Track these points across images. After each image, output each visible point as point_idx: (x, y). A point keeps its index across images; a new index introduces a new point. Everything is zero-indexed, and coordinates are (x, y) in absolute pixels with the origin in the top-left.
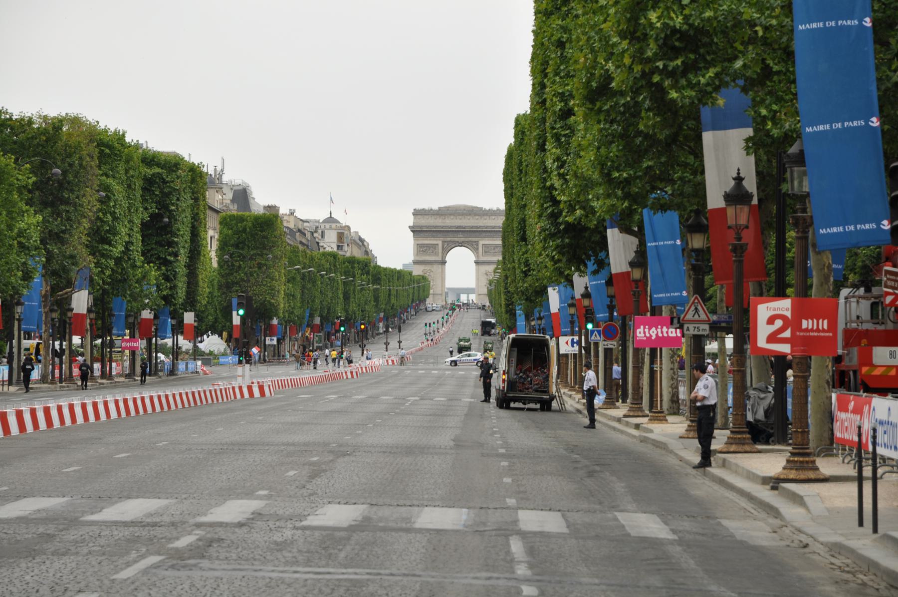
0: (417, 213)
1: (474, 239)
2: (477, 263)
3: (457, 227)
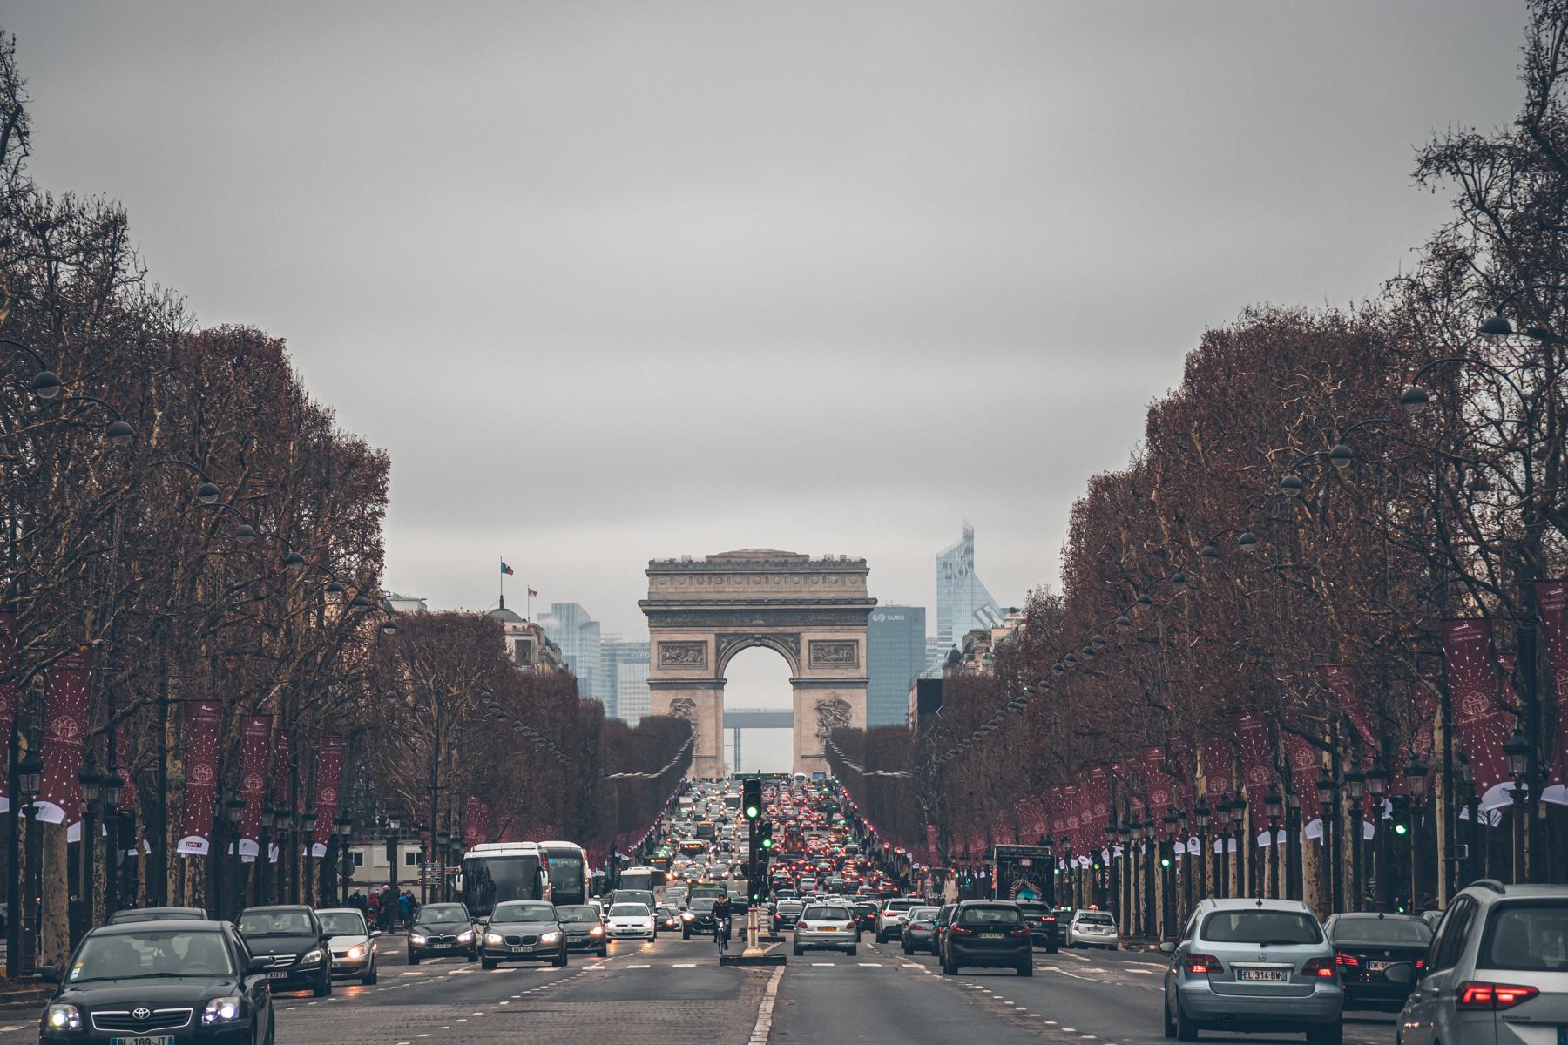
0: (657, 570)
1: (789, 630)
2: (797, 684)
3: (751, 602)
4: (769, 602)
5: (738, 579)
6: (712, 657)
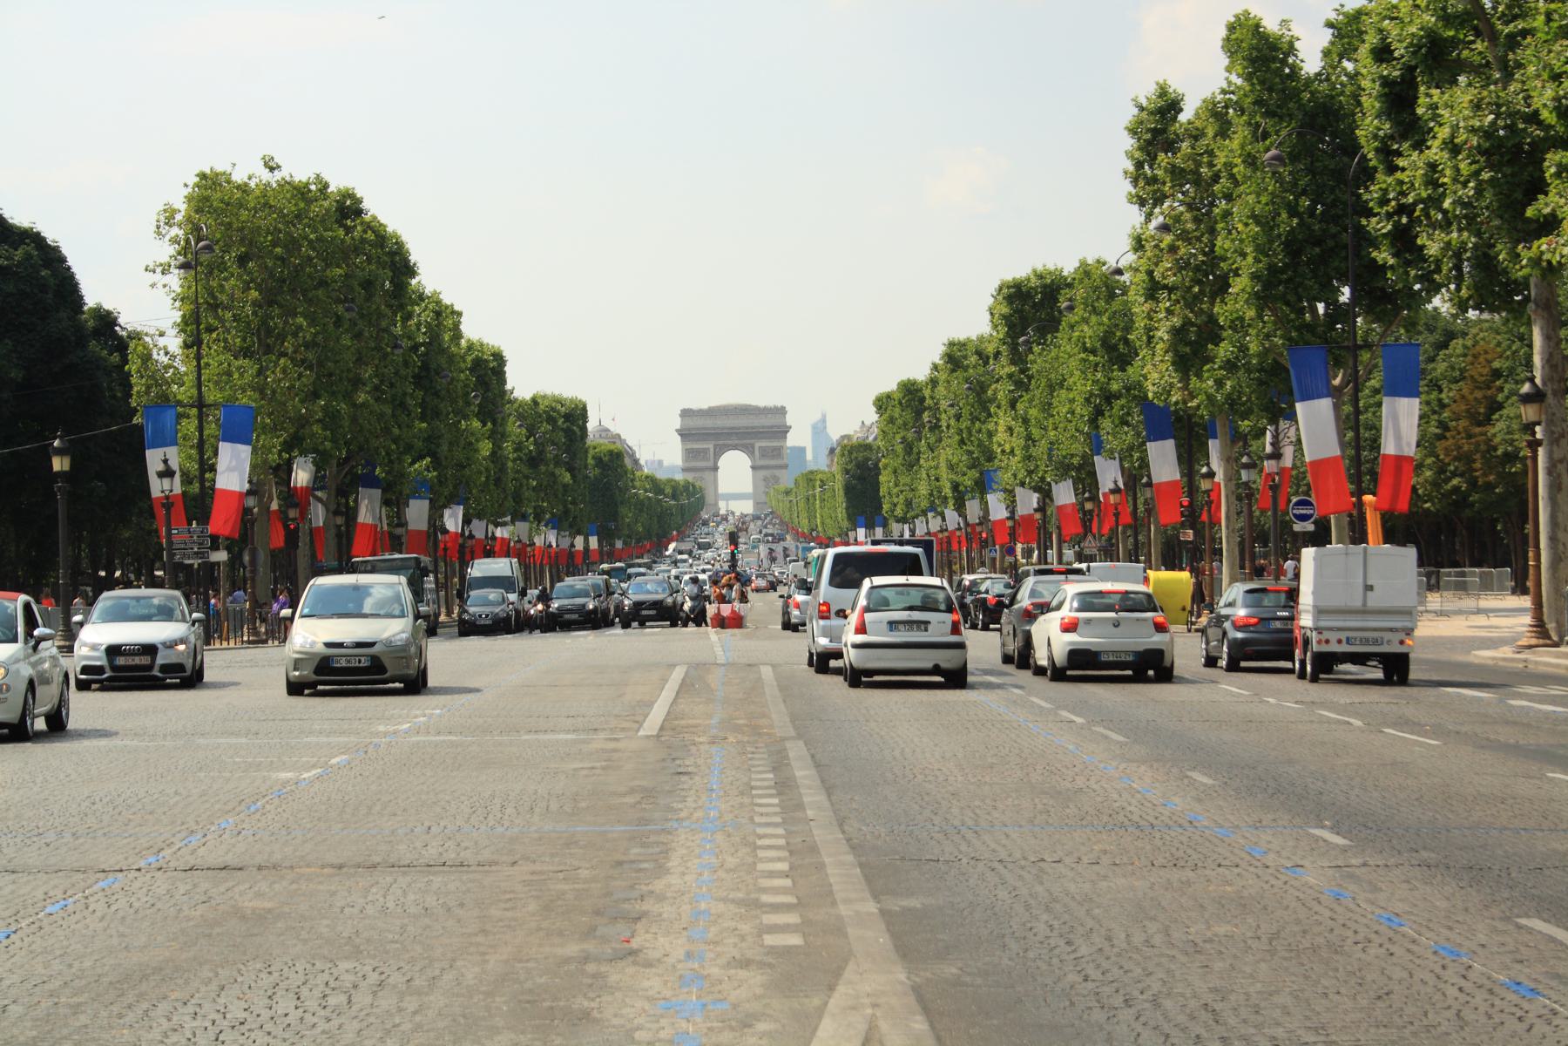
0: (686, 413)
2: (753, 468)
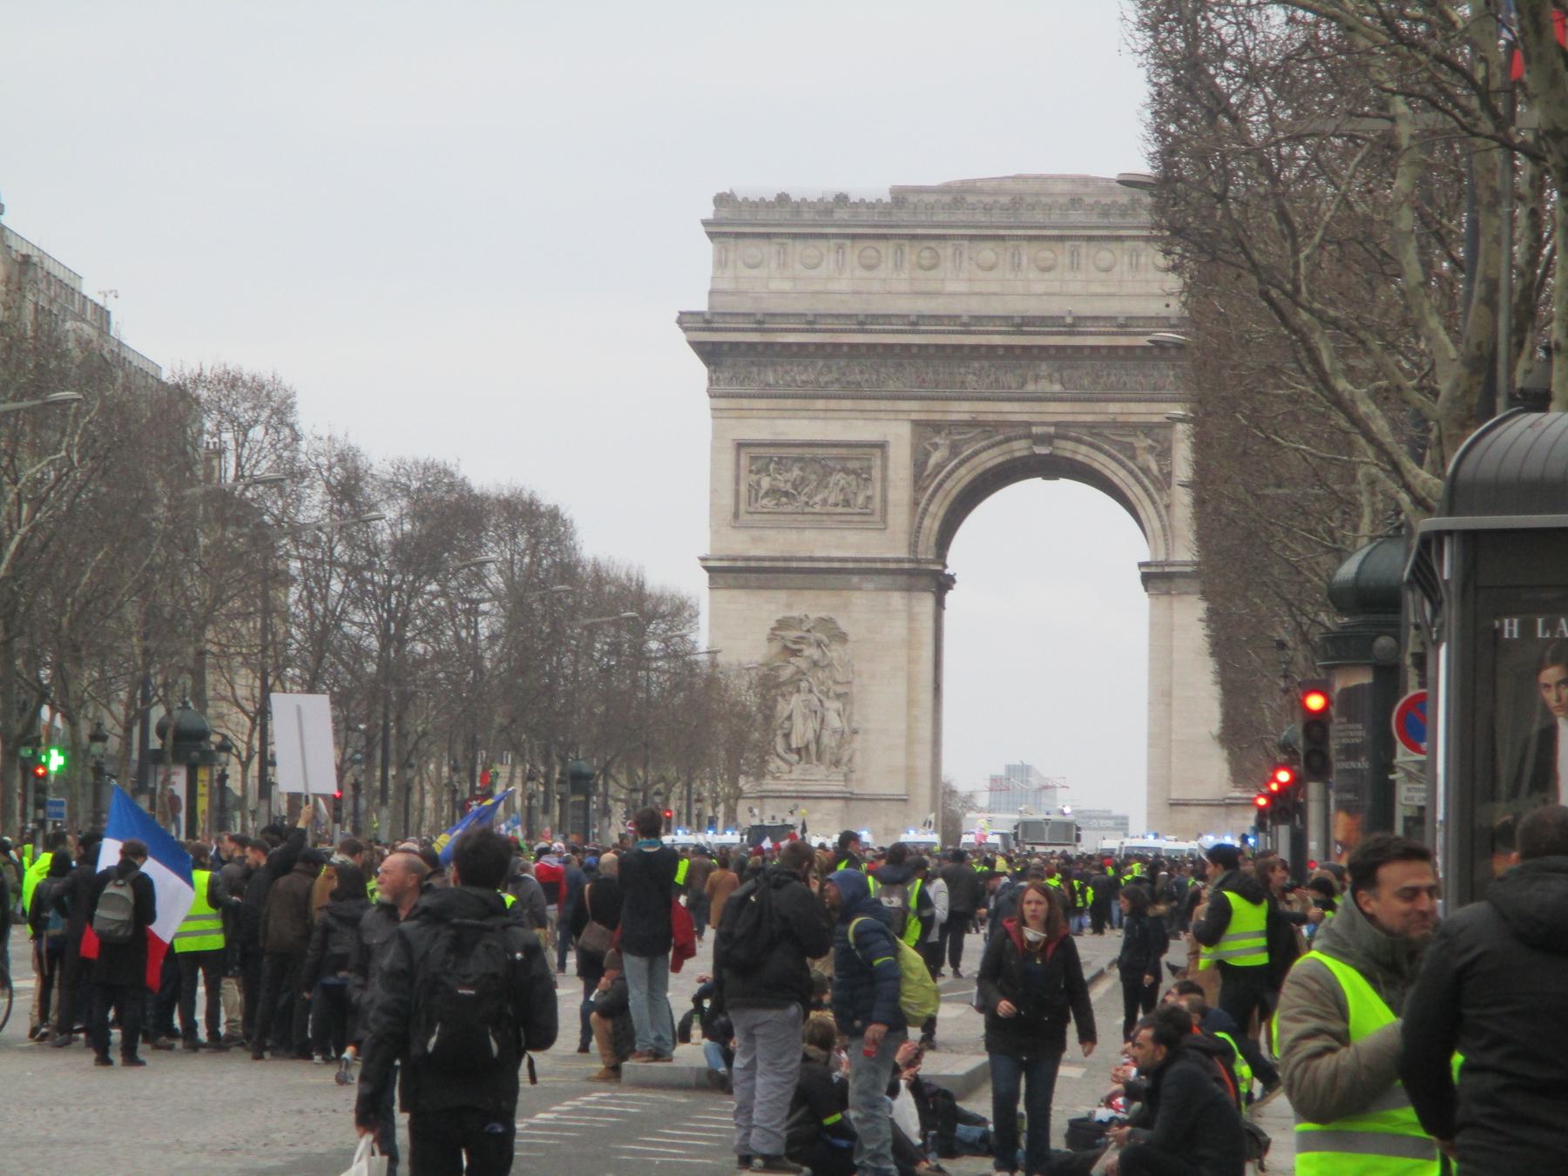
1: (1139, 411)
3: (1022, 324)
4: (1076, 324)
5: (987, 252)
6: (900, 492)
